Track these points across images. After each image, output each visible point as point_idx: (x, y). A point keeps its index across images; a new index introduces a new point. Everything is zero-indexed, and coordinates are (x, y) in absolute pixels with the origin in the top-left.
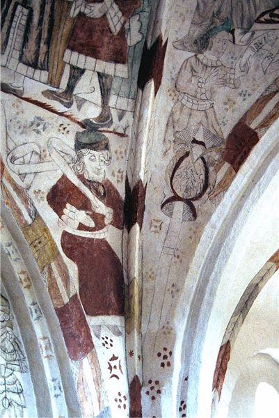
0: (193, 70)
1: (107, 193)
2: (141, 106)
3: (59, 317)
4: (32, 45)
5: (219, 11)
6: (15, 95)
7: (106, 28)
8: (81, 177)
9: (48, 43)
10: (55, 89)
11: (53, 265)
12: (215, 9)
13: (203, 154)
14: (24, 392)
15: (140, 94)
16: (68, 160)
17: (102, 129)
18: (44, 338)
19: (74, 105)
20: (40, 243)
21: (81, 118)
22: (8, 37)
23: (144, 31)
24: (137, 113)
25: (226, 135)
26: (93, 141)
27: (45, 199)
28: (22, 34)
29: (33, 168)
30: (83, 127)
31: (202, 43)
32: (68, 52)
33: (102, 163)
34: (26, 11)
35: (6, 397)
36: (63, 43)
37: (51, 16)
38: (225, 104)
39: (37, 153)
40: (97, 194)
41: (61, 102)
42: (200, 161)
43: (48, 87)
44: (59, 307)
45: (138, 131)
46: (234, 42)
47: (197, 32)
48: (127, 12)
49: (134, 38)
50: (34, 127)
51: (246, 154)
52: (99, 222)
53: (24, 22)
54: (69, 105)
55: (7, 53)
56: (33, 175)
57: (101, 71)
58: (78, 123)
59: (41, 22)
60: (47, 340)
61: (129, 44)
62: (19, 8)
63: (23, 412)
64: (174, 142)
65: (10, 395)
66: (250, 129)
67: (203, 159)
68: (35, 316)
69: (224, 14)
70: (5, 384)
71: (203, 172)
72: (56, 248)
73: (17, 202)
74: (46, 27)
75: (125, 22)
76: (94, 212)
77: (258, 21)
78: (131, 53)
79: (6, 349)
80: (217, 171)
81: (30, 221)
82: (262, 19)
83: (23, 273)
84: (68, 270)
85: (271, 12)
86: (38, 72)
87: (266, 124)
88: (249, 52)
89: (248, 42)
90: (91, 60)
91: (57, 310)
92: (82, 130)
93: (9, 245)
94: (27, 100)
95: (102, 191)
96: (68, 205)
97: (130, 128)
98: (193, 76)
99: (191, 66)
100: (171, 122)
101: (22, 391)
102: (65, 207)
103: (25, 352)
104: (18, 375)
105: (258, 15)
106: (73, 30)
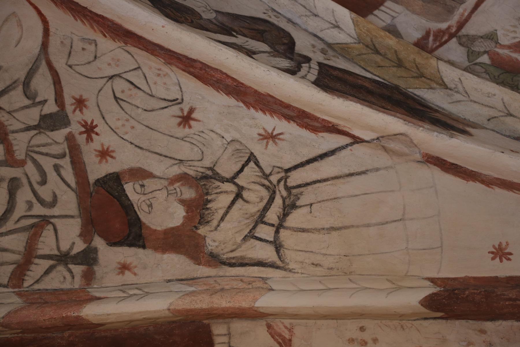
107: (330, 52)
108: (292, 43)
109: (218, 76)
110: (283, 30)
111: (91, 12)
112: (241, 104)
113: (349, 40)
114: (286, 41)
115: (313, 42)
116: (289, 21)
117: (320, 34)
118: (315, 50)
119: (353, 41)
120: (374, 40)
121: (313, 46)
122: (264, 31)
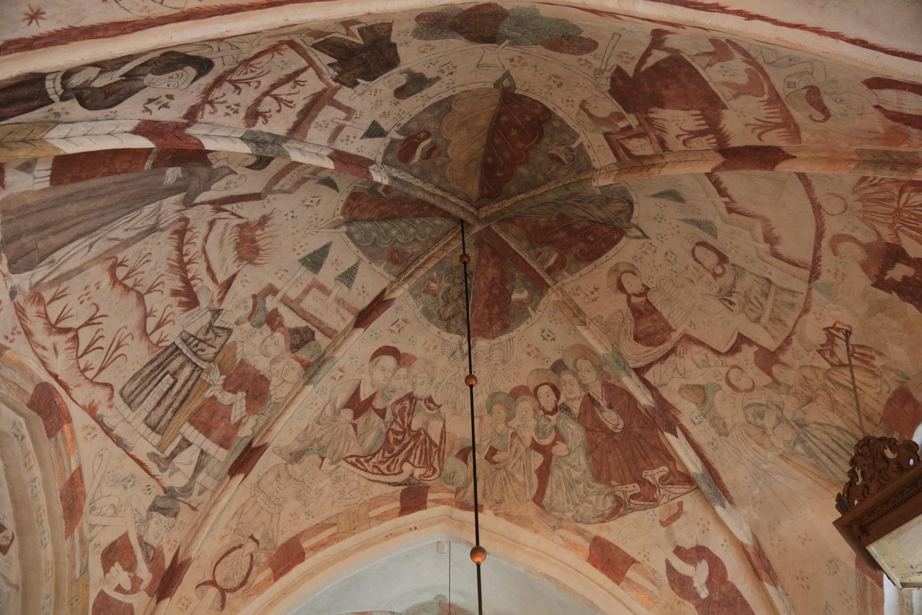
0: (278, 475)
1: (154, 556)
2: (223, 491)
4: (160, 411)
5: (321, 439)
6: (124, 450)
7: (227, 416)
8: (140, 538)
9: (175, 412)
10: (159, 453)
12: (318, 436)
13: (254, 552)
15: (226, 483)
16: (137, 519)
17: (180, 498)
19: (168, 472)
21: (167, 483)
22: (145, 398)
23: (256, 431)
24: (217, 495)
25: (279, 544)
26: (167, 507)
27: (100, 553)
28: (158, 398)
29: (104, 520)
30: (165, 492)
31: (296, 457)
32: (187, 424)
33: (164, 529)
34: (171, 381)
36: (187, 415)
37: (189, 391)
38: (291, 515)
39: (114, 507)
40: (147, 557)
41: (159, 465)
42: (249, 557)
43: (155, 450)
45: (209, 512)
46: (320, 467)
47: (297, 447)
48: (250, 410)
49: (245, 432)
50: (125, 483)
51: (289, 568)
52: (136, 582)
53: (165, 389)
54: (163, 470)
55: (137, 412)
56: (100, 528)
57: (204, 449)
58: (163, 488)
59: (179, 392)
61: (239, 434)
62: (168, 376)
64: (235, 531)
66: (301, 547)
67: (252, 556)
69: (323, 442)
71: (247, 569)
74: (180, 398)
75: (244, 417)
76: (135, 575)
77: (345, 459)
78: (236, 442)
80: (259, 572)
82: (349, 460)
85: (358, 457)
86: (154, 434)
87: (315, 549)
88: (328, 481)
89: (330, 473)
90: (202, 437)
92: (162, 494)
94: (132, 457)
95: (151, 554)
96: (117, 564)
97: (204, 505)
98: (276, 480)
99: (279, 472)
100: (240, 513)
102: (113, 565)
105: (349, 454)
106: (200, 408)
107: (52, 118)
108: (82, 103)
109: (110, 33)
110: (95, 109)
111: (218, 15)
112: (77, 26)
113: (49, 135)
114: (87, 101)
115: (69, 116)
116: (97, 120)
117: (70, 125)
118: (64, 111)
119: (46, 136)
120: (33, 147)
121: (67, 113)
122: (106, 98)
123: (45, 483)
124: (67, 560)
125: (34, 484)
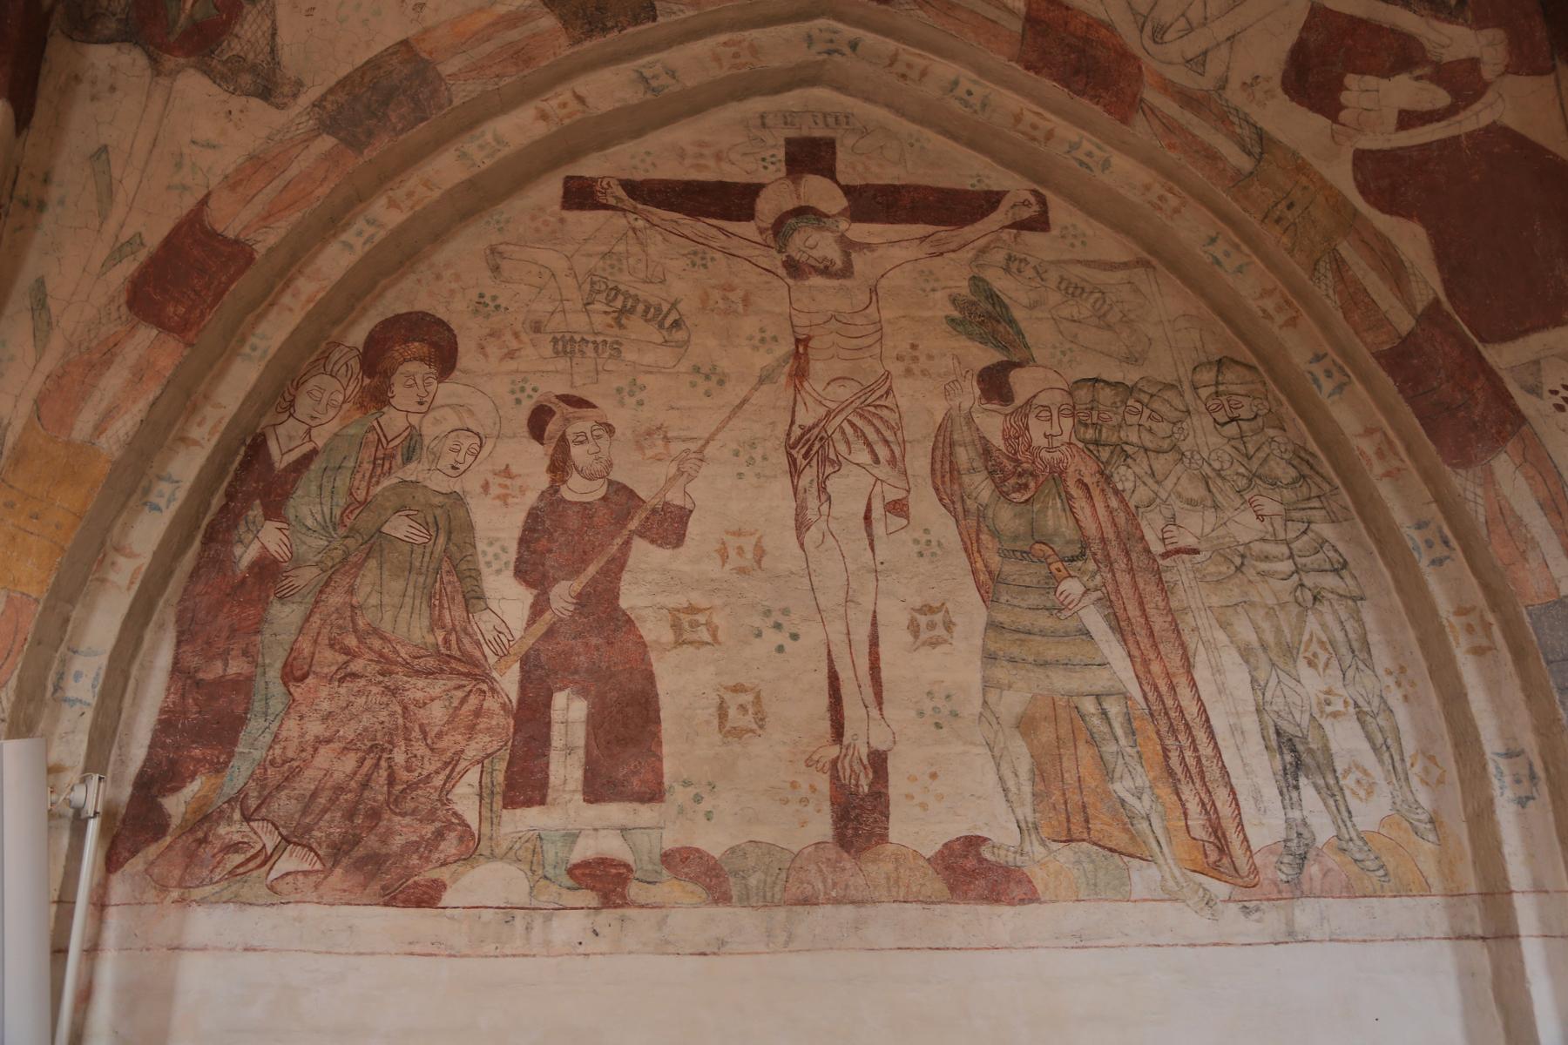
3: (1392, 373)
11: (1345, 249)
14: (1352, 564)
18: (1369, 432)
20: (1290, 206)
27: (1279, 91)
35: (1302, 585)
44: (1386, 347)
56: (1224, 50)
60: (1378, 436)
63: (1359, 612)
65: (1309, 580)
68: (1327, 385)
70: (1291, 556)
72: (1345, 202)
73: (1197, 132)
79: (1277, 478)
81: (1246, 164)
83: (1266, 293)
84: (1394, 247)
91: (1378, 356)
93: (1213, 240)
96: (1351, 80)
101: (1345, 565)
102: (1341, 87)
103: (1332, 474)
104: (1327, 531)
123: (982, 71)
124: (1173, 155)
125: (960, 91)
